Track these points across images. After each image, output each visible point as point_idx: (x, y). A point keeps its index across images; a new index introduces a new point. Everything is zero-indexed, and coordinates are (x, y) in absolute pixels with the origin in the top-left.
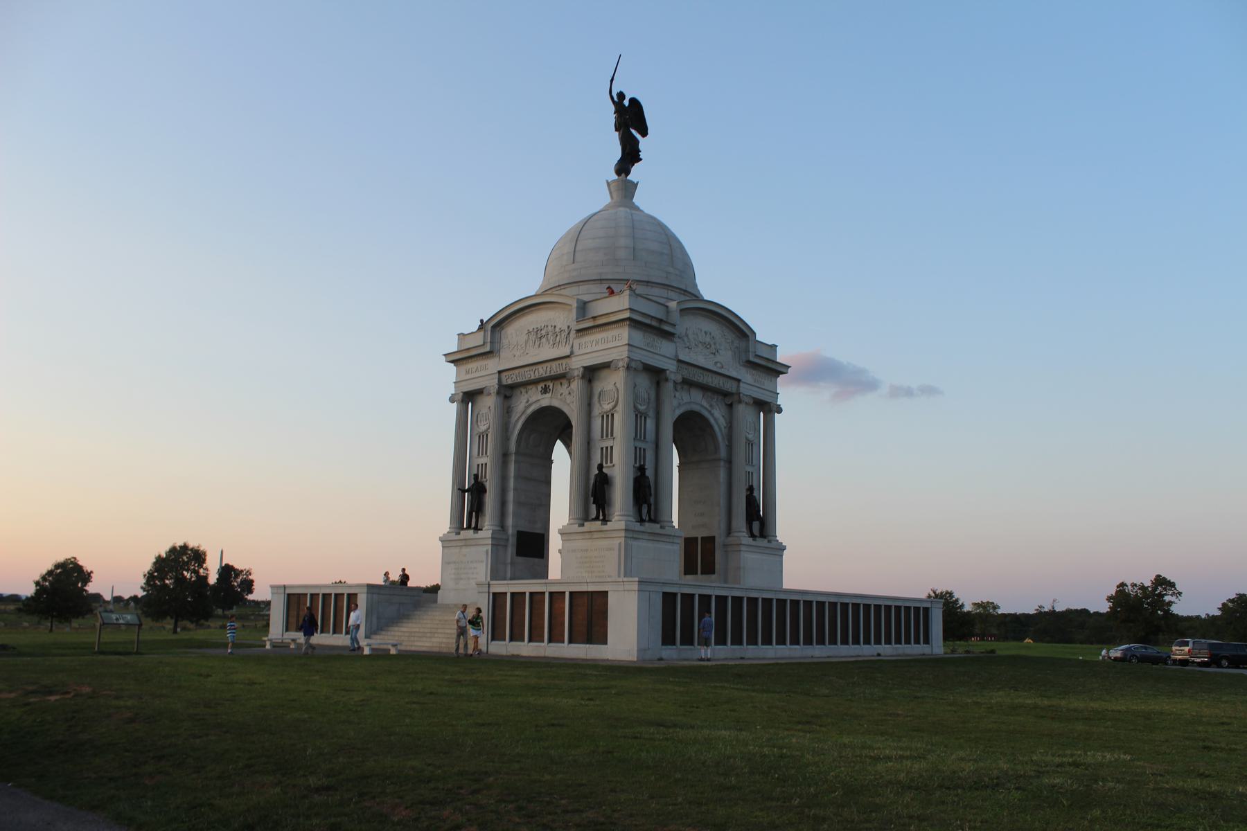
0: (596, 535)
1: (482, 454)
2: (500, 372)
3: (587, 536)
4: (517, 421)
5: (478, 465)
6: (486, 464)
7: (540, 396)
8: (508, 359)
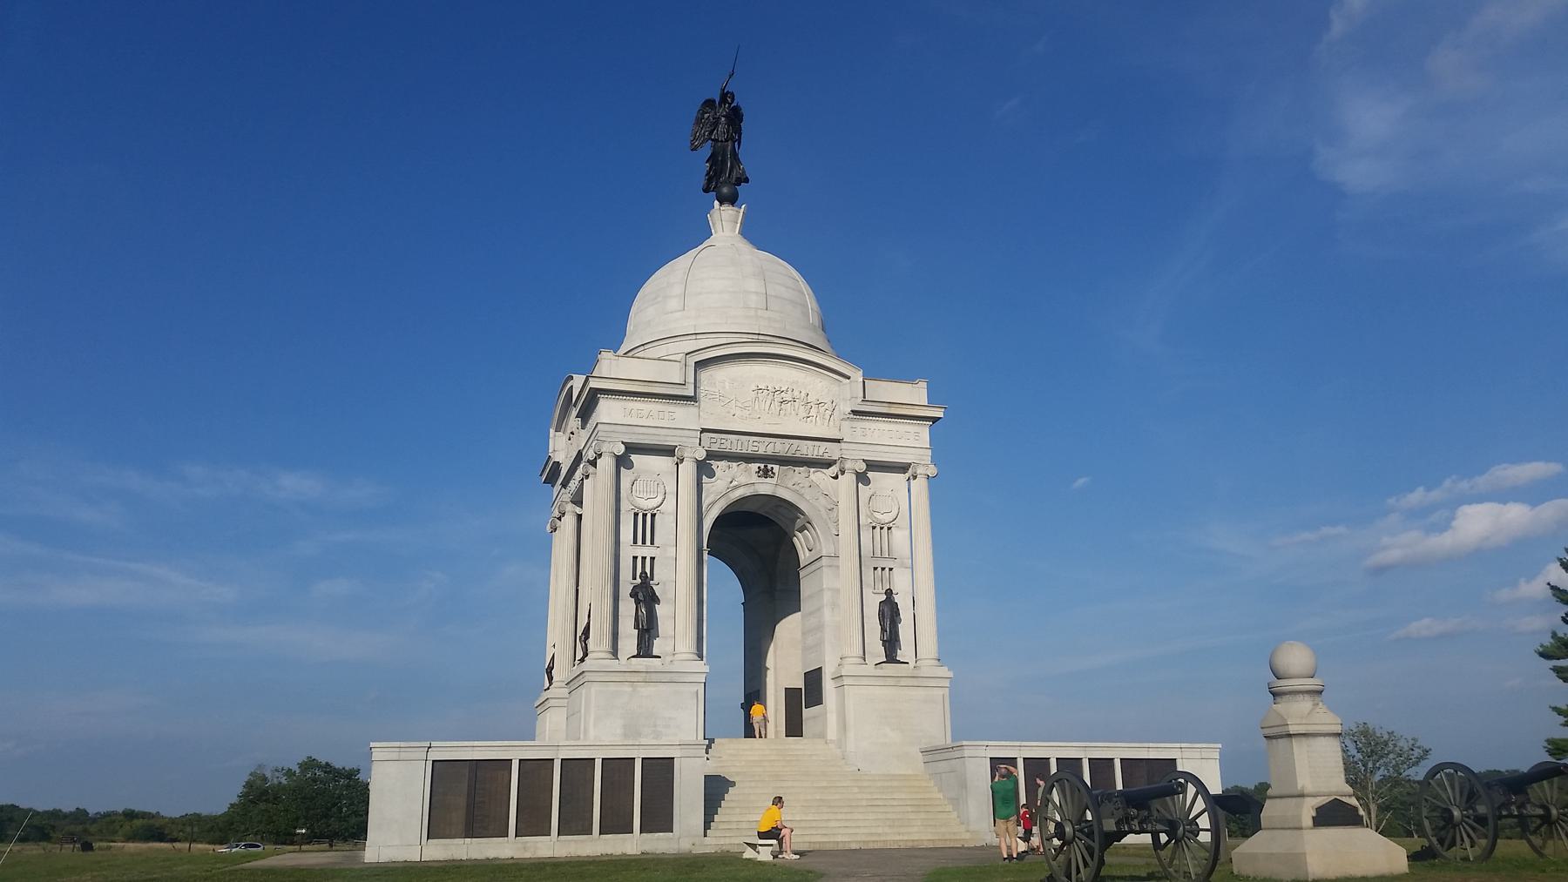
0: (903, 682)
1: (644, 542)
2: (704, 431)
3: (891, 681)
4: (714, 503)
5: (635, 558)
6: (653, 559)
7: (755, 479)
8: (710, 414)
